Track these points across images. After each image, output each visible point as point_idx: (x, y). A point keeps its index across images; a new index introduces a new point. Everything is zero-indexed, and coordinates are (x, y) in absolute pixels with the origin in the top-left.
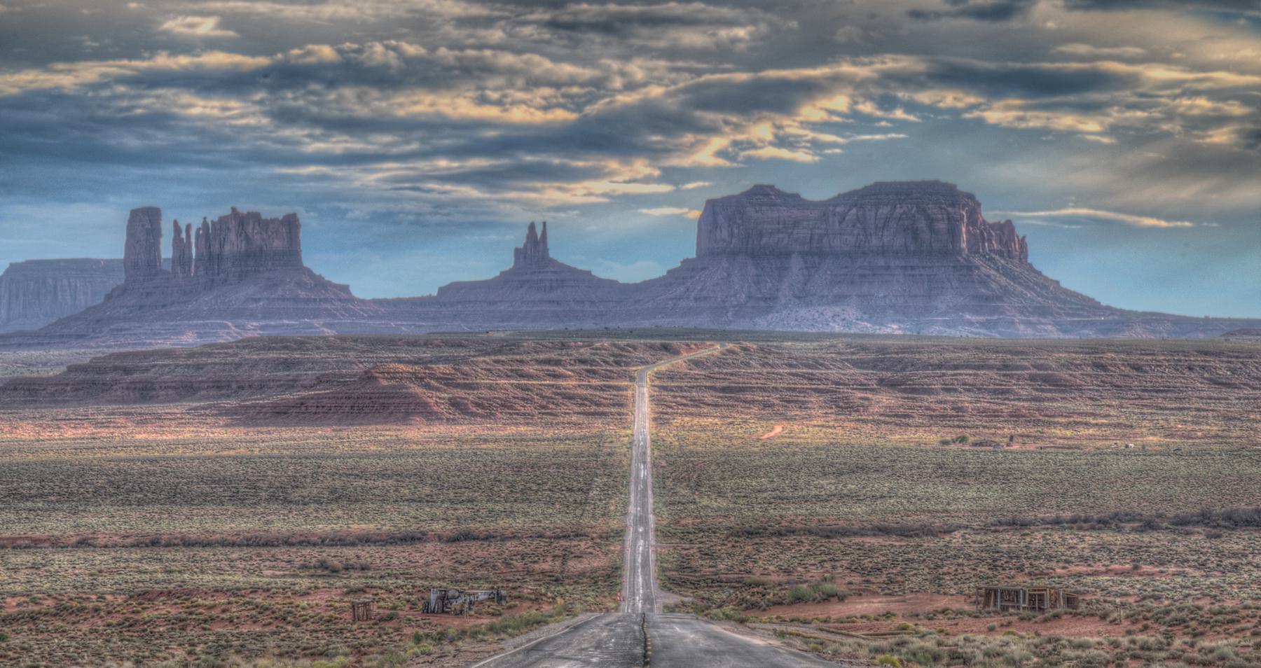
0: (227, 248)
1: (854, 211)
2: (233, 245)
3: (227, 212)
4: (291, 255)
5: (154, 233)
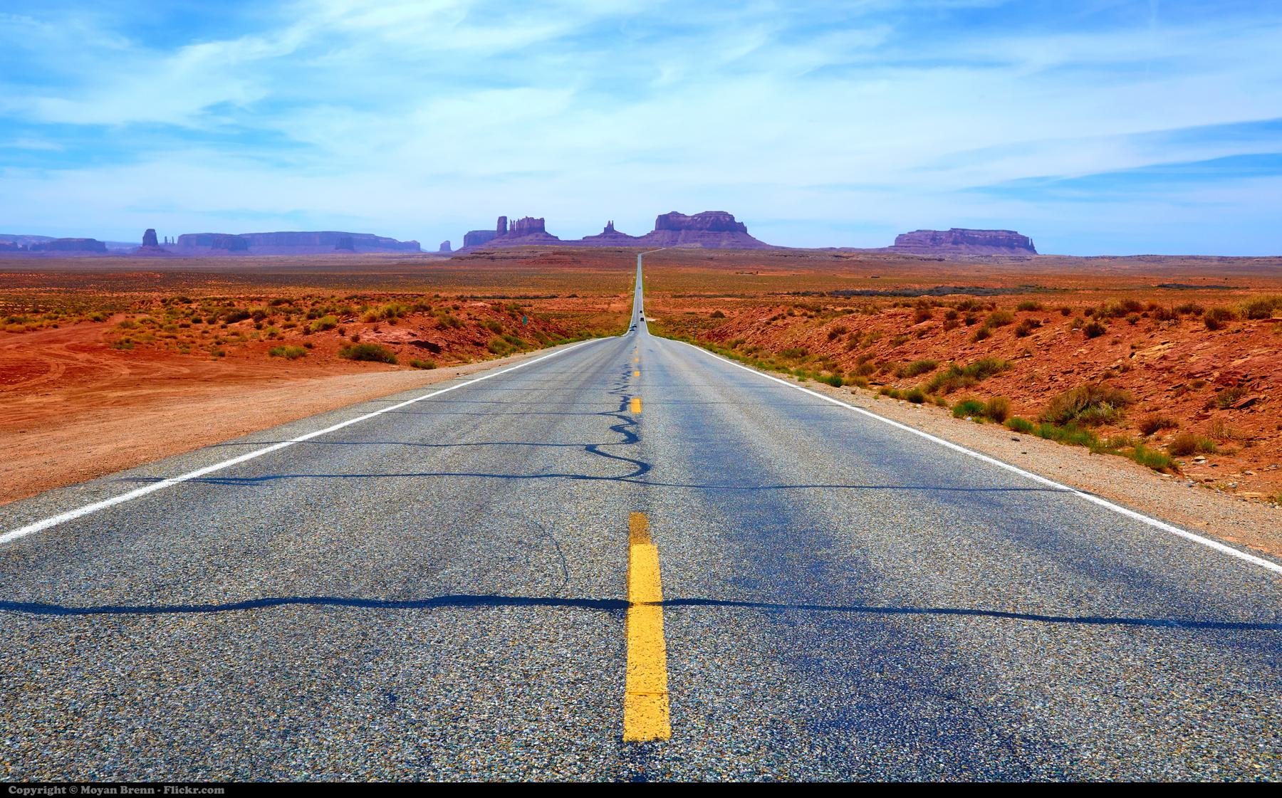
5: (505, 223)
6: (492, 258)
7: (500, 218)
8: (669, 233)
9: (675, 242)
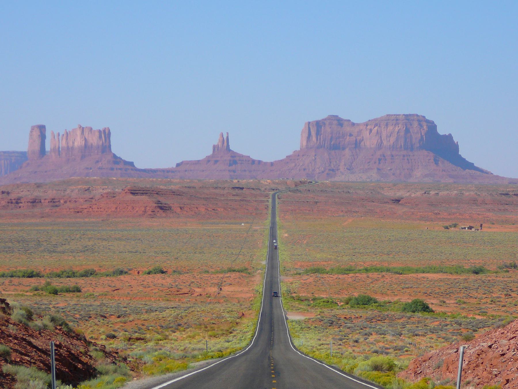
0: (76, 144)
1: (376, 128)
2: (79, 142)
4: (106, 148)
5: (43, 137)
7: (33, 128)
9: (333, 171)
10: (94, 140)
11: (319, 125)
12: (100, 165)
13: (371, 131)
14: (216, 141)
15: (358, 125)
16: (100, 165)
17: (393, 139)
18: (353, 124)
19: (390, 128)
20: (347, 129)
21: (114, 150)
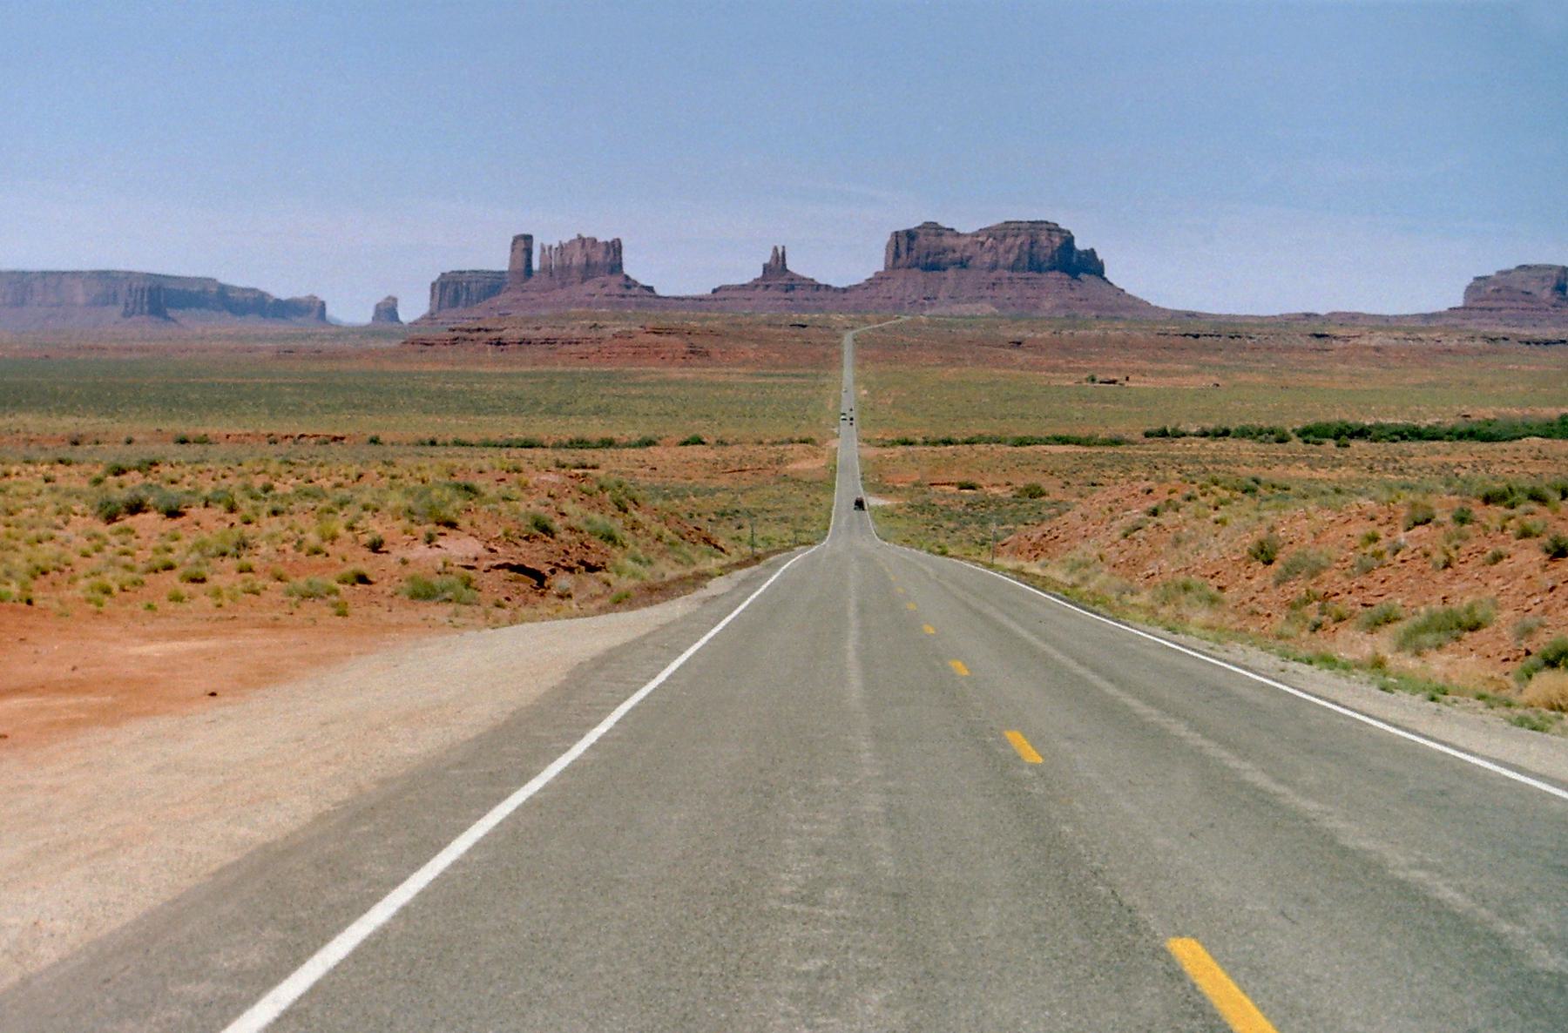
0: (575, 261)
2: (578, 259)
3: (574, 237)
4: (616, 267)
5: (528, 252)
6: (499, 343)
7: (516, 239)
8: (919, 276)
10: (599, 256)
11: (911, 235)
12: (606, 290)
13: (983, 244)
14: (767, 258)
15: (965, 235)
16: (606, 290)
17: (1012, 257)
18: (958, 235)
19: (1009, 241)
20: (948, 241)
21: (627, 270)
